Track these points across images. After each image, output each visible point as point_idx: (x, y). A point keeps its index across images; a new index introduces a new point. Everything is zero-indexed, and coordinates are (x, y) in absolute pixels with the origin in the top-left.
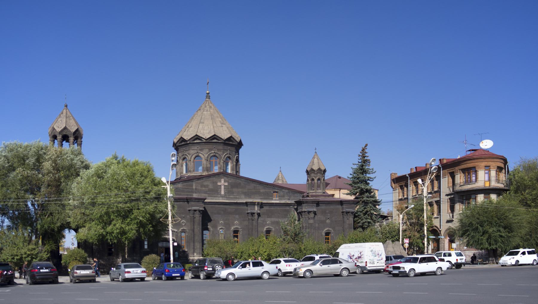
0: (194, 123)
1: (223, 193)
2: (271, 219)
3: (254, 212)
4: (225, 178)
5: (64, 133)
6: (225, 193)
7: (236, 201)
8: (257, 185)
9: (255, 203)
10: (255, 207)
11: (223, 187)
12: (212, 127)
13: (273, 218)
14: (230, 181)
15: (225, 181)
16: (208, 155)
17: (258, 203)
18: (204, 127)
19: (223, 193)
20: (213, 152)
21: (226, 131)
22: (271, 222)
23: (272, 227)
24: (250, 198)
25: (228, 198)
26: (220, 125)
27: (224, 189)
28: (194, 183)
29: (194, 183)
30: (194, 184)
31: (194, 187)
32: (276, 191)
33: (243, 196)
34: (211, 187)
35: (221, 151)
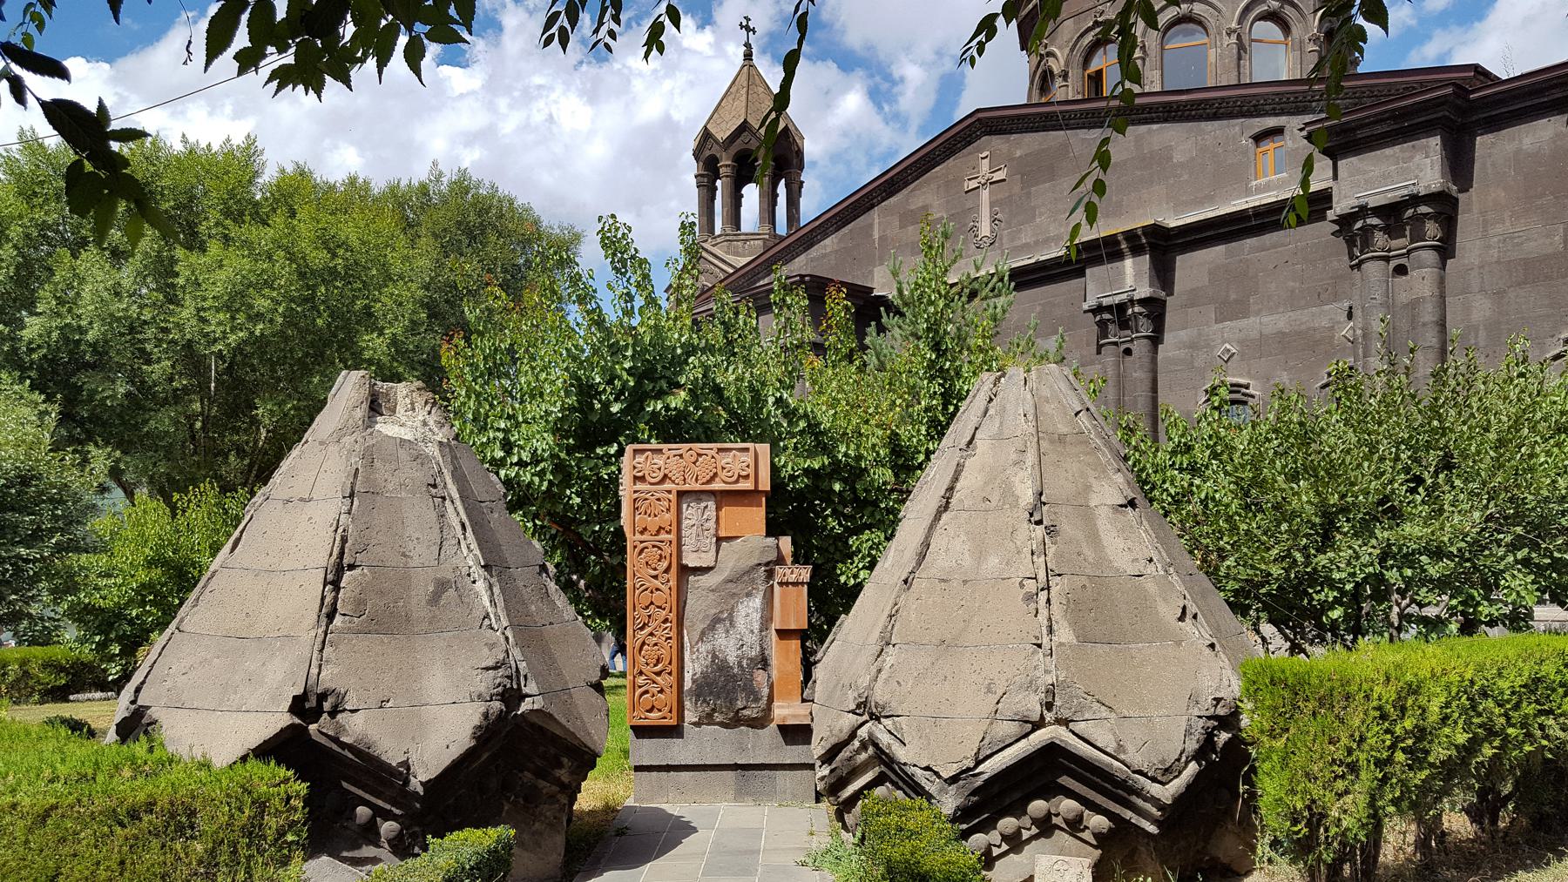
1: (985, 229)
3: (1117, 300)
4: (997, 143)
5: (707, 153)
7: (1032, 261)
8: (1155, 127)
9: (1111, 241)
10: (1122, 273)
13: (1258, 313)
14: (1018, 153)
17: (1130, 236)
19: (985, 229)
22: (1241, 342)
23: (1249, 375)
27: (992, 205)
30: (876, 221)
31: (876, 236)
32: (1271, 122)
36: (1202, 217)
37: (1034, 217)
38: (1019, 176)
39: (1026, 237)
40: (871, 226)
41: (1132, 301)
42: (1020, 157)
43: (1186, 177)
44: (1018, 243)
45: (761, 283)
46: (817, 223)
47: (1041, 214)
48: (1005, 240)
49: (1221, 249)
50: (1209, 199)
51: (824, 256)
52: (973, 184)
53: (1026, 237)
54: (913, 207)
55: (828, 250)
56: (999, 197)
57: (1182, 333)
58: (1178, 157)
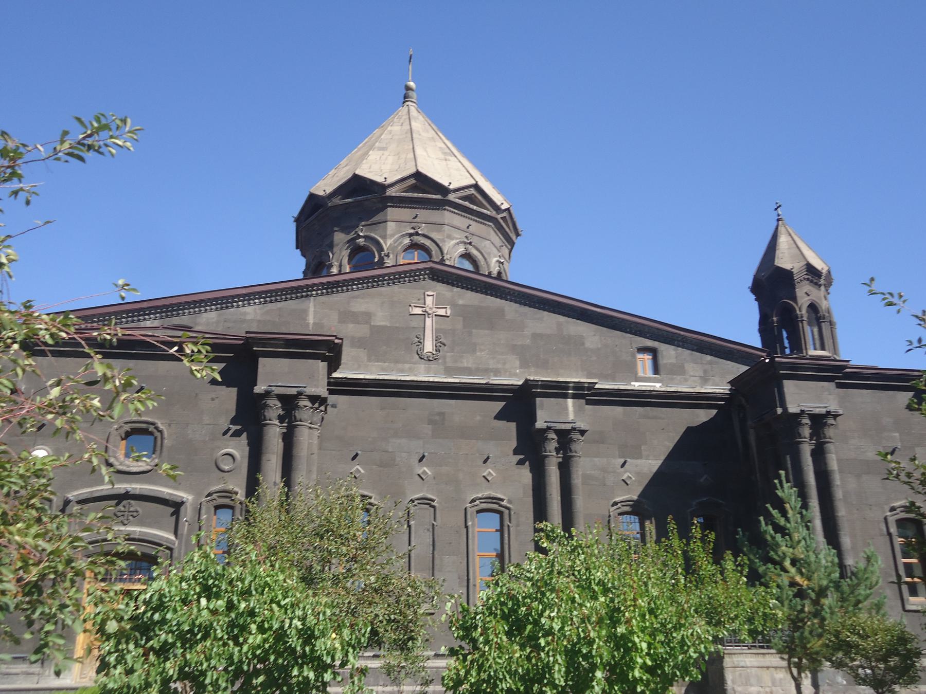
0: (356, 153)
1: (429, 346)
2: (639, 461)
3: (563, 427)
4: (442, 288)
6: (439, 345)
7: (484, 382)
9: (563, 386)
10: (566, 409)
11: (429, 321)
12: (411, 155)
14: (461, 302)
15: (439, 303)
16: (395, 242)
17: (579, 386)
18: (383, 157)
19: (429, 346)
20: (412, 231)
21: (458, 170)
24: (543, 365)
25: (449, 371)
26: (442, 156)
27: (438, 330)
28: (311, 305)
29: (311, 305)
30: (312, 309)
31: (311, 320)
33: (514, 362)
34: (381, 319)
35: (439, 231)
36: (616, 387)
37: (474, 351)
38: (461, 318)
39: (468, 362)
40: (305, 312)
41: (574, 429)
42: (463, 306)
43: (594, 358)
44: (460, 365)
45: (148, 324)
46: (244, 291)
47: (481, 351)
48: (448, 360)
49: (619, 409)
50: (613, 379)
51: (244, 321)
52: (418, 311)
53: (468, 362)
54: (354, 309)
55: (249, 317)
56: (443, 327)
57: (596, 459)
58: (588, 344)
